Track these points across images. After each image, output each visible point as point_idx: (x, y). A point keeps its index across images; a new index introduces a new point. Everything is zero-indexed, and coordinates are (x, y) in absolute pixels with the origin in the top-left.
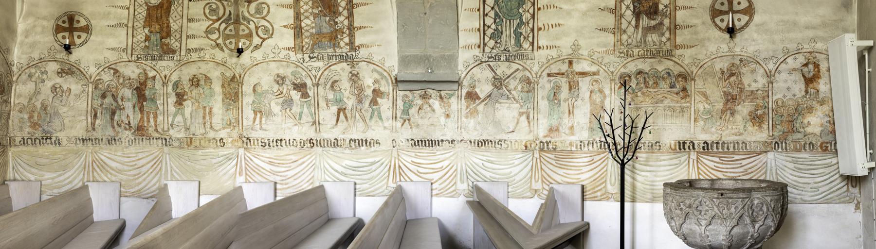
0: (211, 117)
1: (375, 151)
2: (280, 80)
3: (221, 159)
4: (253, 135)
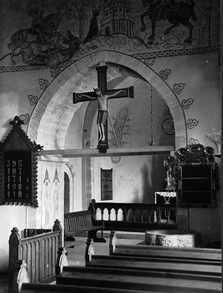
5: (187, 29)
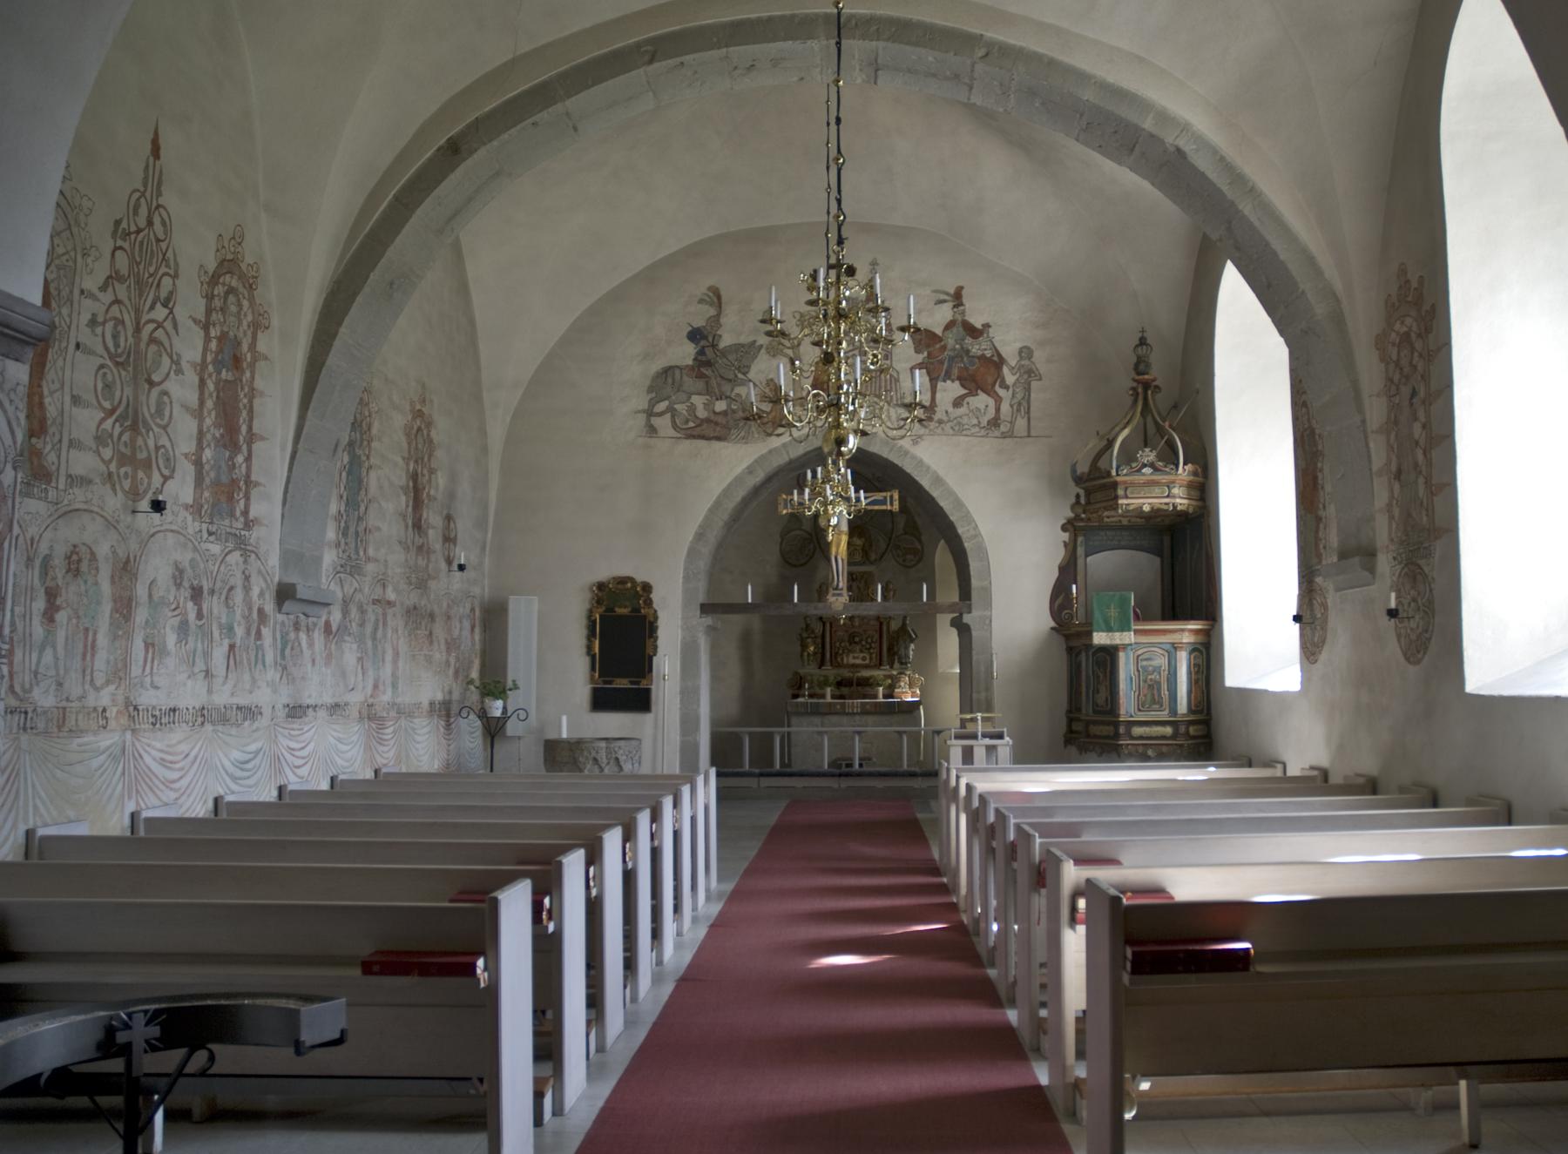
0: (93, 655)
1: (257, 730)
2: (178, 575)
3: (103, 757)
4: (147, 698)
5: (991, 402)
